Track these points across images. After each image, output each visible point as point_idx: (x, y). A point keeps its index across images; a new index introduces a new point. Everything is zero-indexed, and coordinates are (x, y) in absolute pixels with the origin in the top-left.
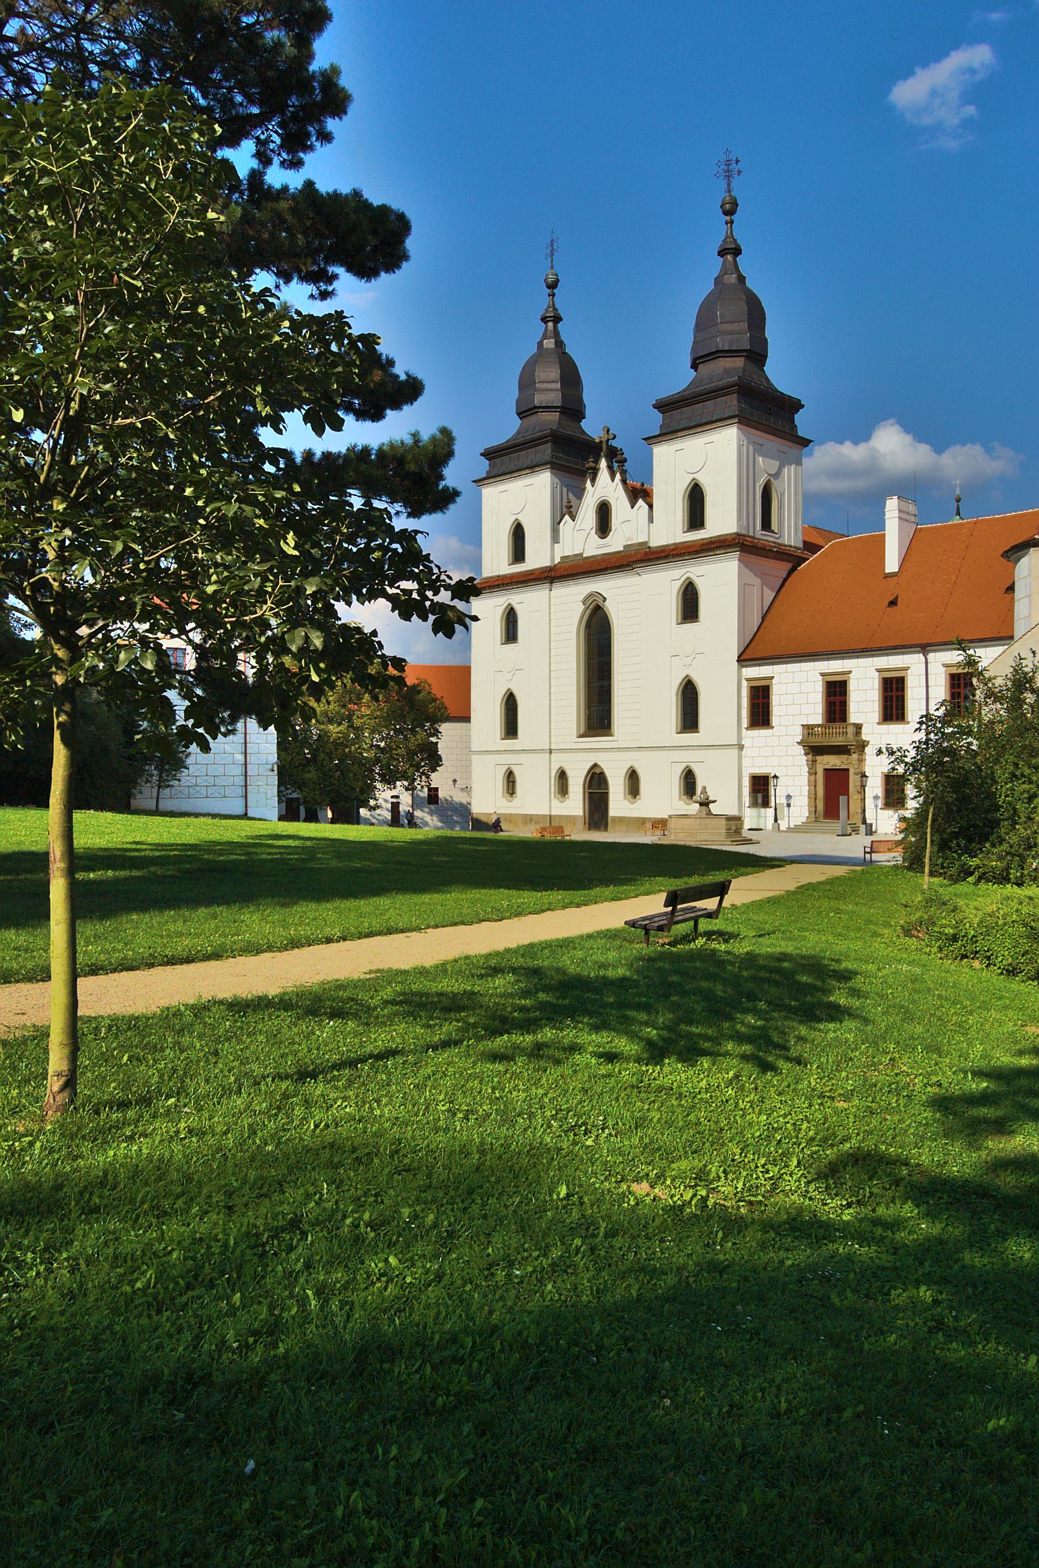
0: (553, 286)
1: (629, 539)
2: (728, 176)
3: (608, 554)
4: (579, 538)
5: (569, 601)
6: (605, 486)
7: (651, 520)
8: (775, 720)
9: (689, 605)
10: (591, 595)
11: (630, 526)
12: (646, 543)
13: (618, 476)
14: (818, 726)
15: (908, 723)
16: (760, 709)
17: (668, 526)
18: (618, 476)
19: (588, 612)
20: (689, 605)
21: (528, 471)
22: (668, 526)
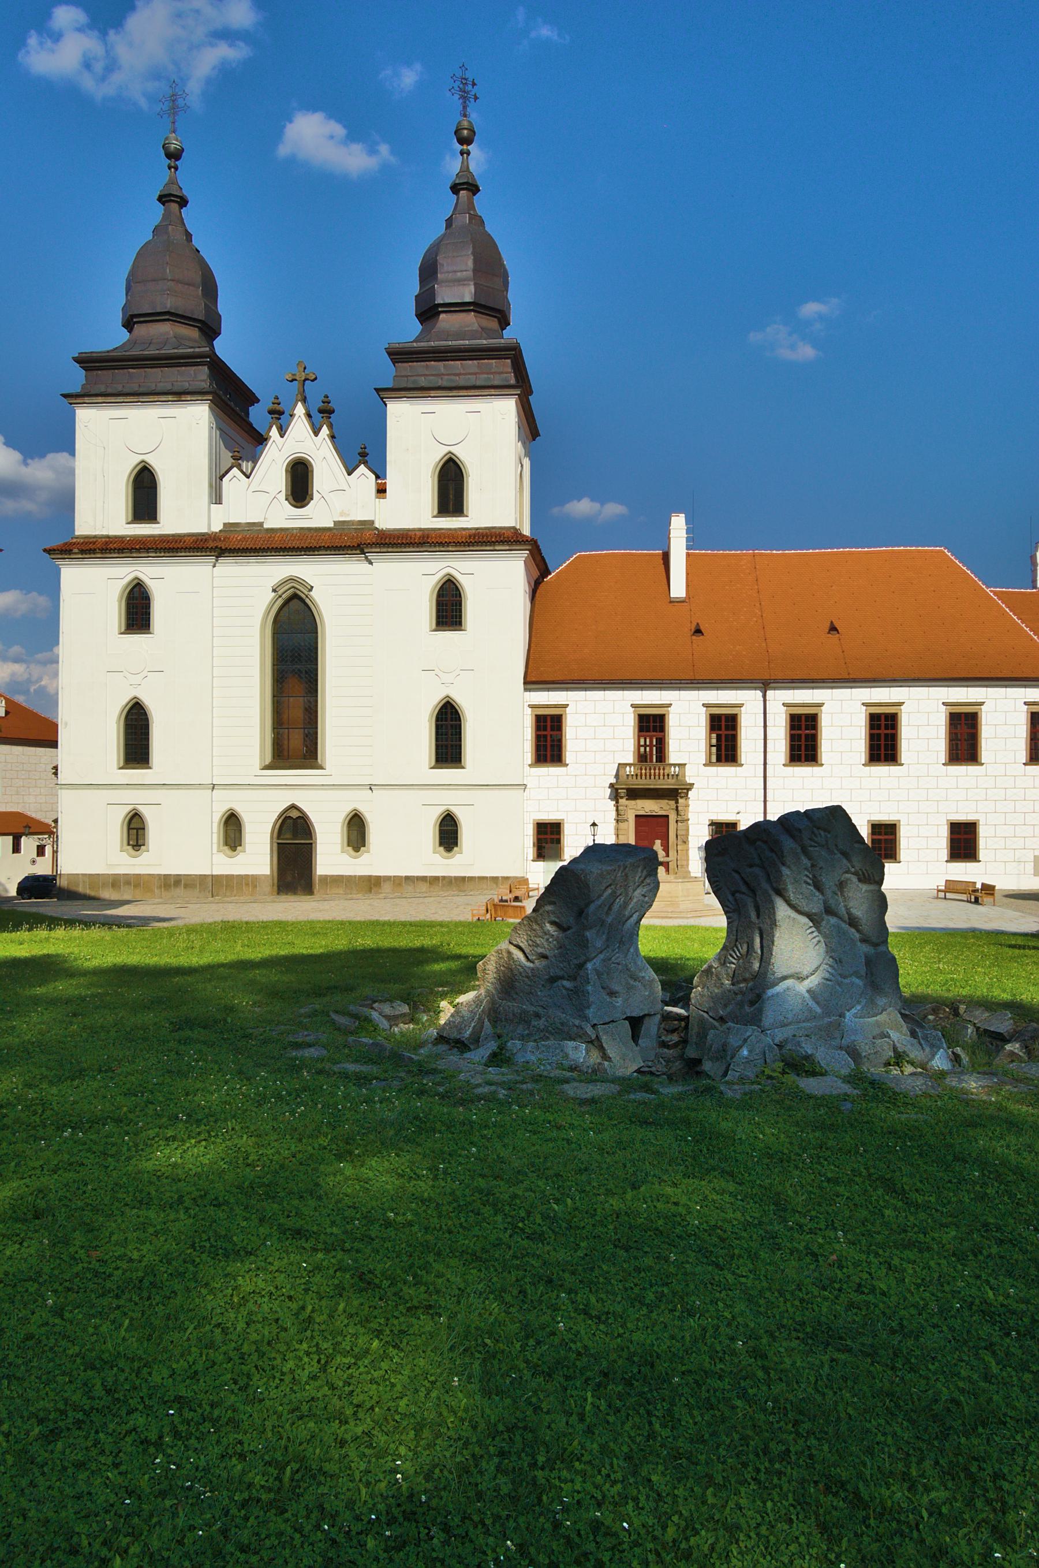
0: (174, 156)
1: (342, 514)
2: (464, 98)
3: (309, 529)
4: (257, 497)
5: (258, 582)
6: (299, 438)
7: (381, 491)
8: (569, 756)
9: (449, 608)
10: (291, 579)
11: (342, 496)
12: (372, 522)
13: (325, 431)
14: (630, 765)
15: (822, 765)
16: (549, 741)
17: (412, 506)
18: (325, 431)
19: (280, 602)
20: (449, 608)
21: (170, 398)
22: (412, 506)
